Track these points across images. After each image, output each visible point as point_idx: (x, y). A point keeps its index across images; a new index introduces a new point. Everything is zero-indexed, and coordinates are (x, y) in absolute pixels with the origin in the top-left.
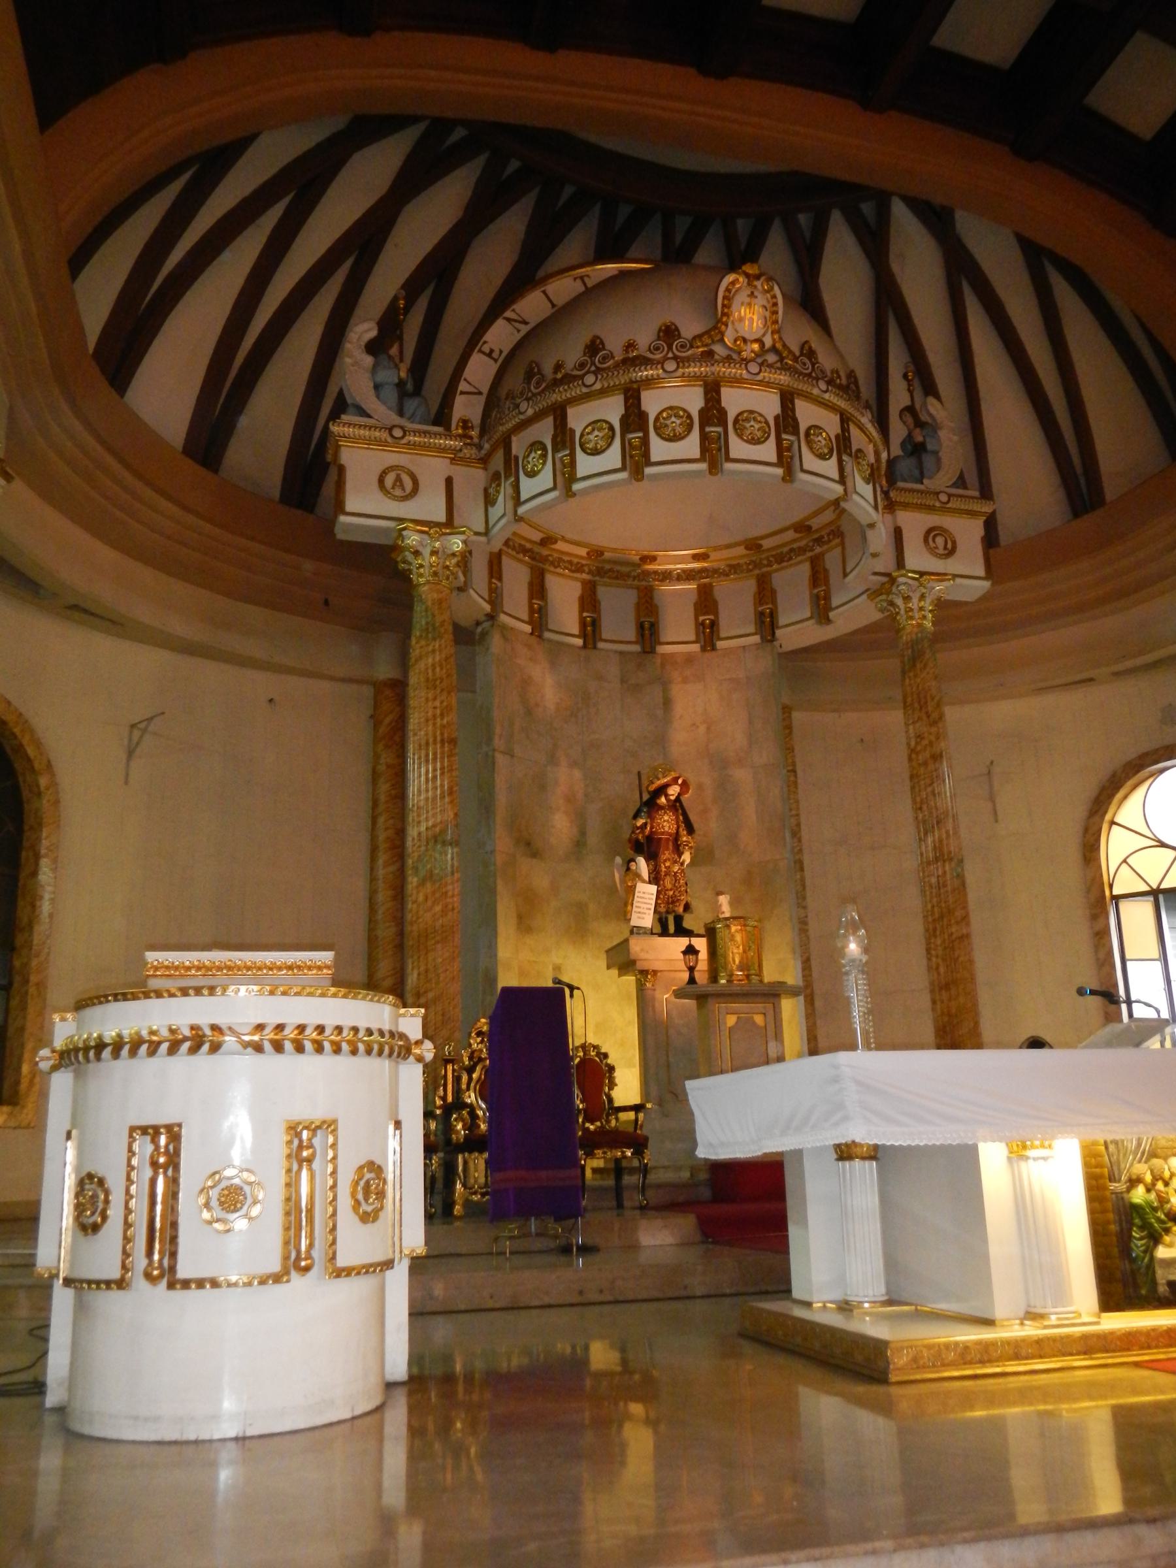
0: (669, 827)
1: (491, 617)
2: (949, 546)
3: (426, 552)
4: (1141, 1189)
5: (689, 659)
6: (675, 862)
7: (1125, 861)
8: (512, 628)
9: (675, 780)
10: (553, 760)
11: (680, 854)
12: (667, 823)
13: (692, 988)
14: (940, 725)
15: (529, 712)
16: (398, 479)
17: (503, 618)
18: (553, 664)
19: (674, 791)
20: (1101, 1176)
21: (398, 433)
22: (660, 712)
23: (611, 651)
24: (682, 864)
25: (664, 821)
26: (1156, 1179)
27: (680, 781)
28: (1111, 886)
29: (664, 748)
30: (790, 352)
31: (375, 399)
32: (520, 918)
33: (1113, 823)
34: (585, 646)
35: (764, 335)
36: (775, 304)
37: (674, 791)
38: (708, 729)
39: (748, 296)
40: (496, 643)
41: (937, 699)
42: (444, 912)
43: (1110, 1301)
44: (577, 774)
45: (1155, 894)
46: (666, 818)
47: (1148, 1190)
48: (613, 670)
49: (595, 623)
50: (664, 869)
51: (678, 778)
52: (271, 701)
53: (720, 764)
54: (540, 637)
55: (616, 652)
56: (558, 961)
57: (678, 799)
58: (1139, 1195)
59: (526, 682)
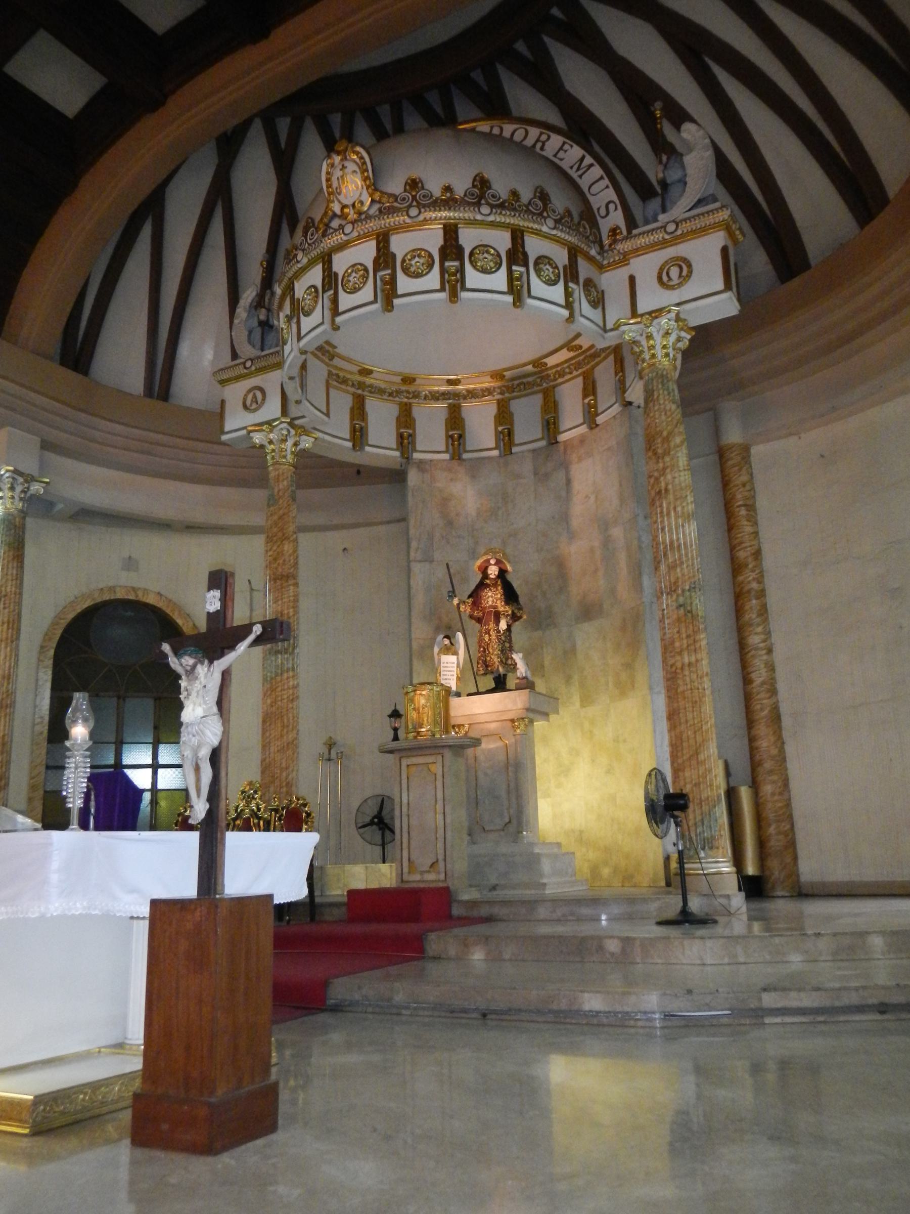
0: (493, 601)
2: (685, 273)
3: (267, 444)
5: (582, 440)
8: (431, 461)
11: (497, 622)
12: (493, 598)
13: (395, 745)
14: (667, 459)
15: (450, 523)
18: (473, 477)
19: (493, 571)
21: (248, 364)
22: (563, 494)
23: (522, 452)
27: (492, 562)
29: (567, 523)
30: (391, 195)
31: (246, 342)
35: (360, 195)
36: (364, 163)
38: (596, 497)
39: (341, 170)
40: (413, 477)
41: (665, 434)
48: (527, 467)
49: (510, 433)
52: (345, 549)
54: (460, 458)
55: (529, 451)
59: (445, 501)
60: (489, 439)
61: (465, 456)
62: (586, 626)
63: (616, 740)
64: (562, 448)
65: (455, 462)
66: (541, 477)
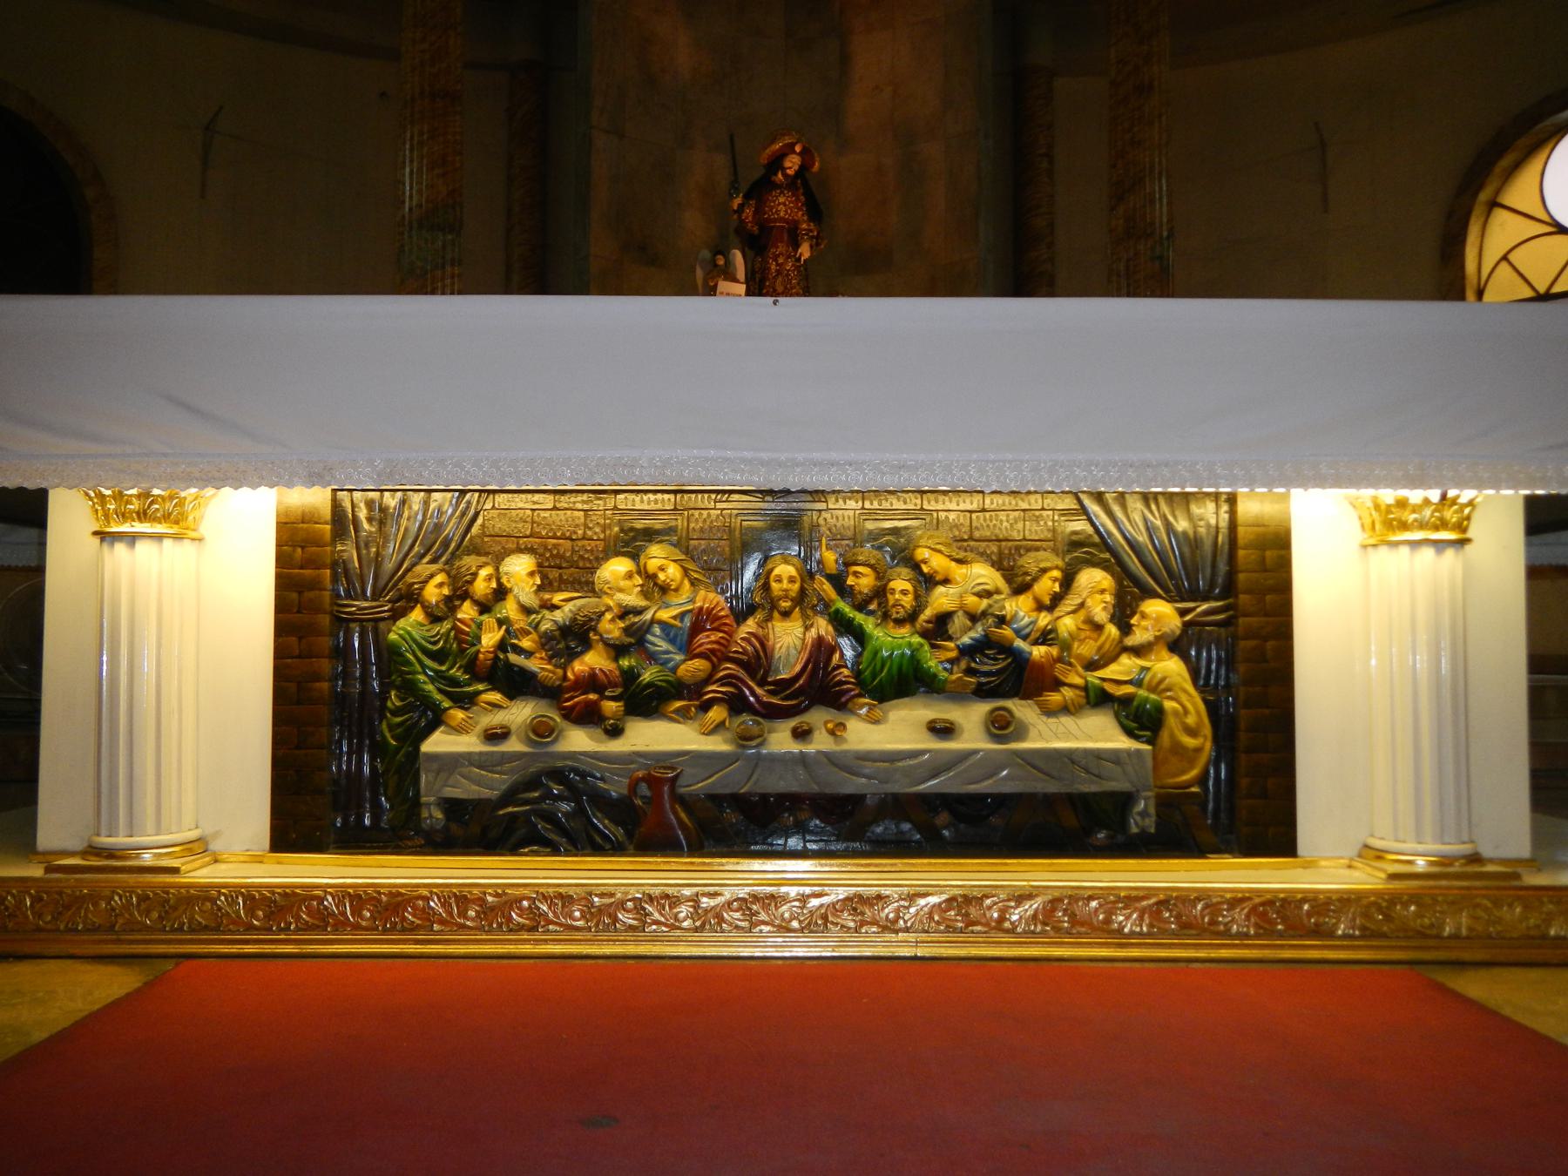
0: (786, 211)
4: (417, 615)
6: (789, 257)
7: (1505, 258)
9: (789, 149)
11: (797, 246)
12: (783, 206)
19: (792, 163)
20: (315, 585)
24: (799, 259)
25: (779, 204)
26: (460, 592)
27: (798, 149)
33: (1494, 204)
37: (792, 163)
46: (782, 200)
47: (434, 619)
50: (773, 267)
51: (796, 143)
52: (383, 94)
57: (799, 173)
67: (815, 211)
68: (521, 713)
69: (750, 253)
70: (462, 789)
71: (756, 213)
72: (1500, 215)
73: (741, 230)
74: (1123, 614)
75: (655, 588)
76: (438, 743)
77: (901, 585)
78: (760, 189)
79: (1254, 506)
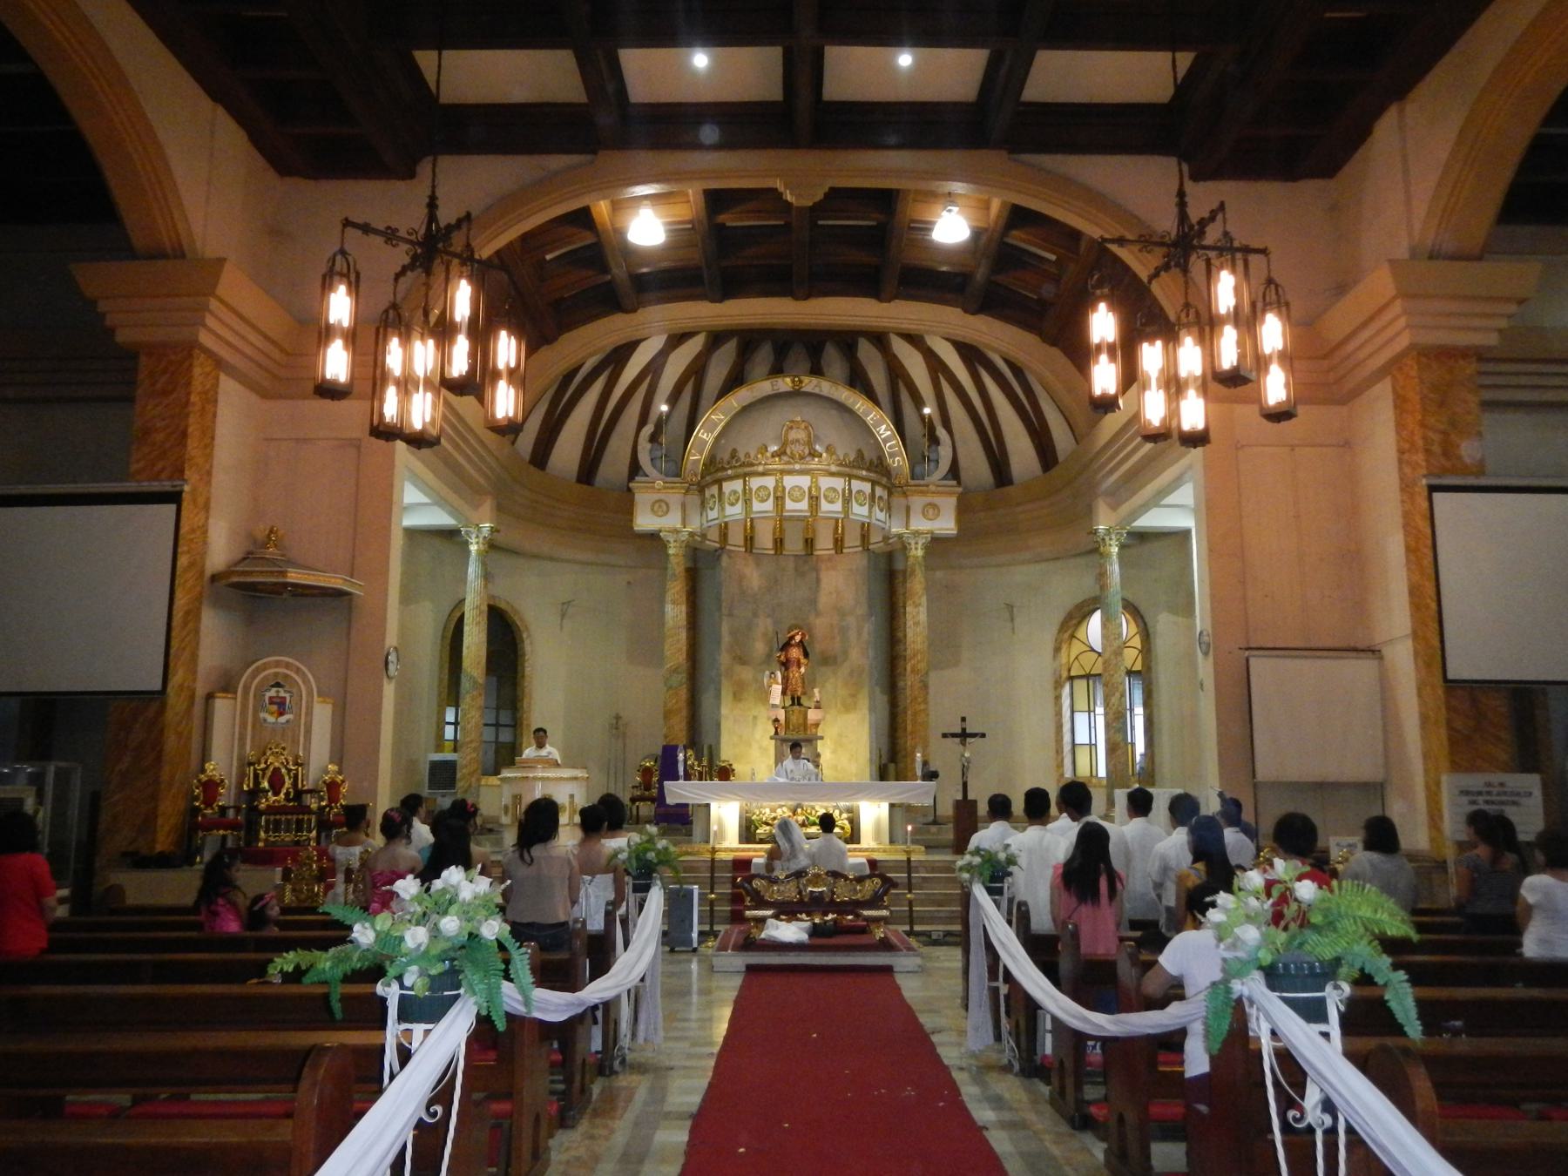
1: (722, 548)
5: (830, 558)
10: (755, 615)
11: (800, 668)
12: (795, 653)
16: (660, 506)
17: (728, 547)
18: (758, 565)
19: (798, 638)
26: (761, 813)
28: (1069, 670)
32: (735, 695)
34: (776, 554)
40: (725, 560)
42: (677, 702)
43: (741, 842)
44: (769, 621)
45: (1087, 677)
48: (791, 565)
53: (842, 614)
54: (751, 552)
56: (756, 714)
57: (801, 641)
58: (754, 817)
59: (741, 578)
60: (770, 544)
61: (754, 551)
62: (823, 669)
63: (840, 735)
64: (815, 558)
65: (747, 555)
66: (799, 573)
67: (806, 655)
68: (768, 828)
69: (783, 669)
70: (762, 837)
71: (786, 656)
72: (1075, 641)
73: (779, 661)
74: (840, 815)
75: (784, 812)
76: (758, 831)
77: (813, 812)
78: (786, 646)
79: (855, 804)
